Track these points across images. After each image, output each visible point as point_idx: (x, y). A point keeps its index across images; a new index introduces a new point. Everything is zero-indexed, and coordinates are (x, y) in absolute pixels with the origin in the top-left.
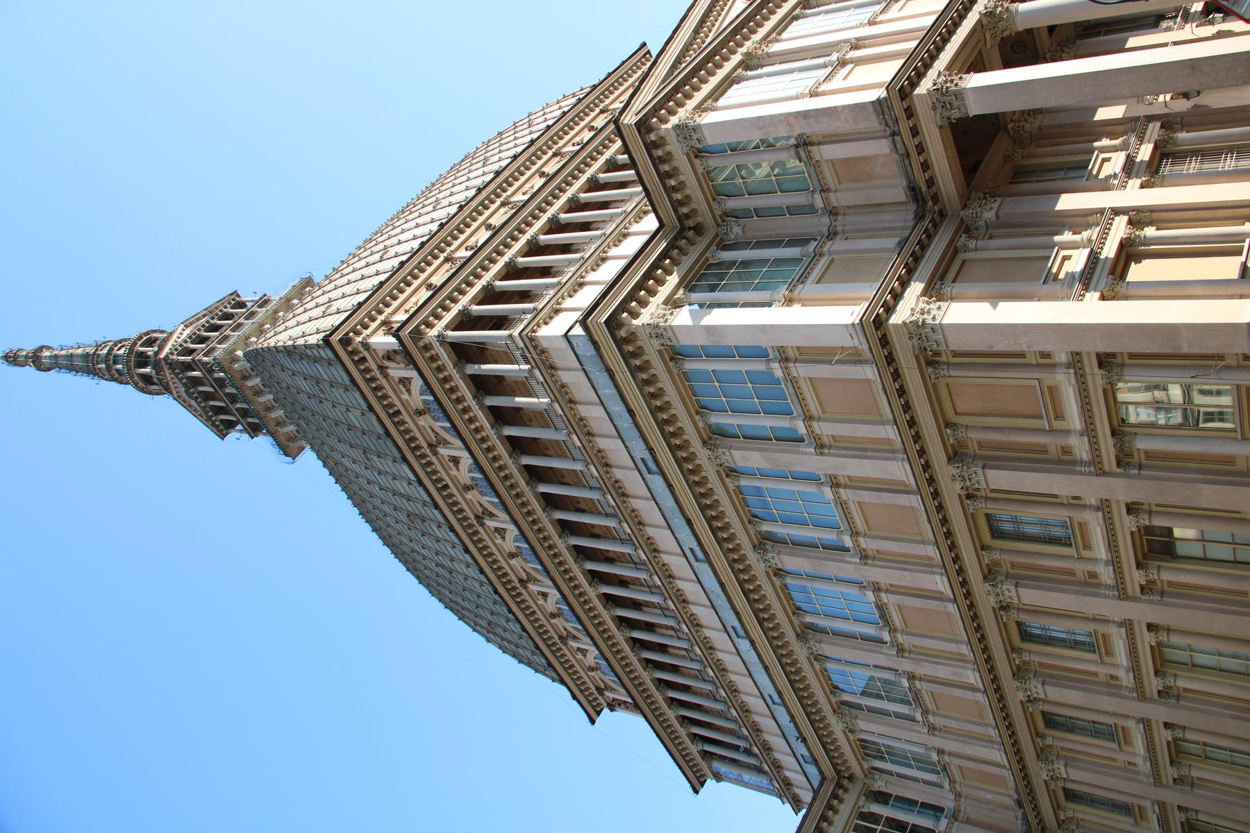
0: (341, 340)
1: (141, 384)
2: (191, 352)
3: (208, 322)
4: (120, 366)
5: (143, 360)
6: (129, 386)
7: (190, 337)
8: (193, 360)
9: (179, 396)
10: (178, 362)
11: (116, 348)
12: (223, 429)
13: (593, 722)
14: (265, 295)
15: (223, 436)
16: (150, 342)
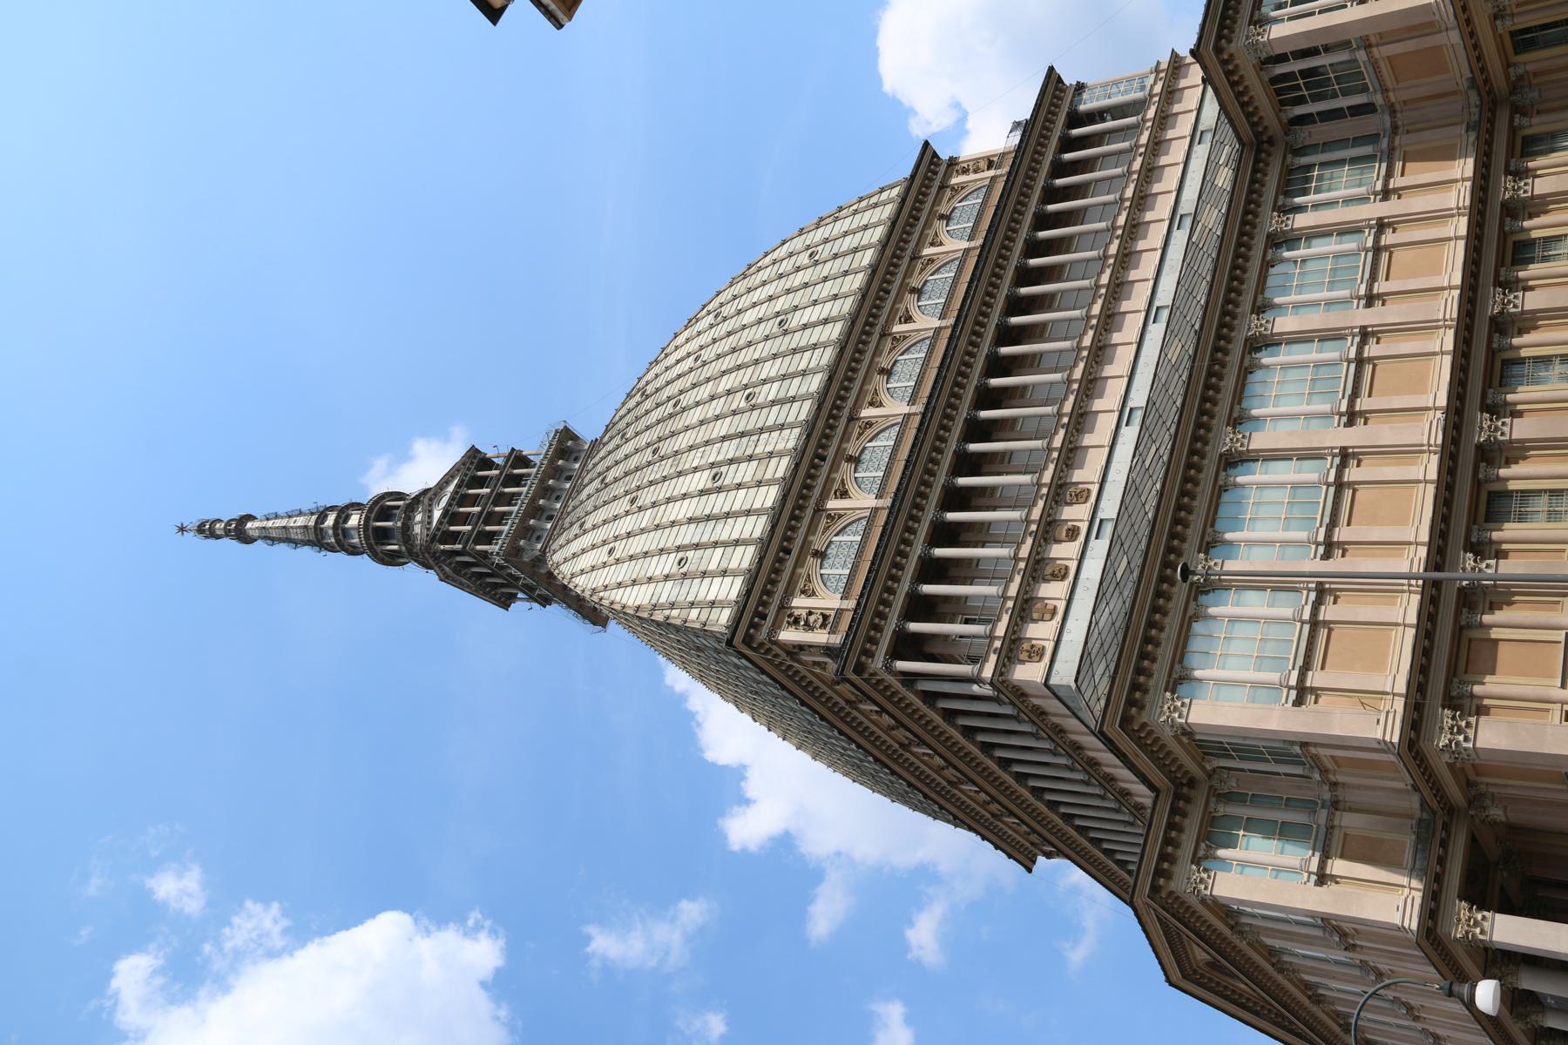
0: (744, 641)
1: (386, 559)
2: (454, 537)
3: (455, 492)
4: (356, 541)
5: (383, 535)
6: (365, 555)
7: (444, 515)
8: (464, 548)
9: (447, 577)
10: (444, 552)
11: (341, 521)
12: (505, 602)
13: (1030, 870)
14: (513, 449)
15: (506, 606)
16: (386, 514)
